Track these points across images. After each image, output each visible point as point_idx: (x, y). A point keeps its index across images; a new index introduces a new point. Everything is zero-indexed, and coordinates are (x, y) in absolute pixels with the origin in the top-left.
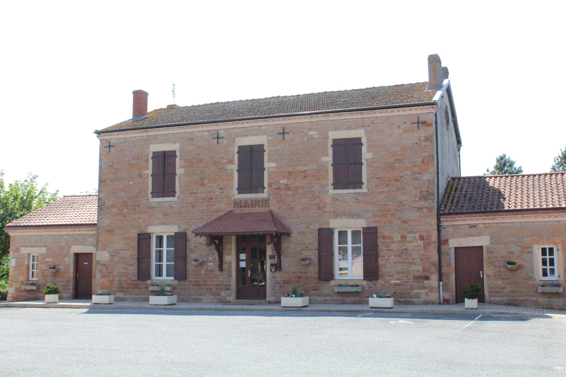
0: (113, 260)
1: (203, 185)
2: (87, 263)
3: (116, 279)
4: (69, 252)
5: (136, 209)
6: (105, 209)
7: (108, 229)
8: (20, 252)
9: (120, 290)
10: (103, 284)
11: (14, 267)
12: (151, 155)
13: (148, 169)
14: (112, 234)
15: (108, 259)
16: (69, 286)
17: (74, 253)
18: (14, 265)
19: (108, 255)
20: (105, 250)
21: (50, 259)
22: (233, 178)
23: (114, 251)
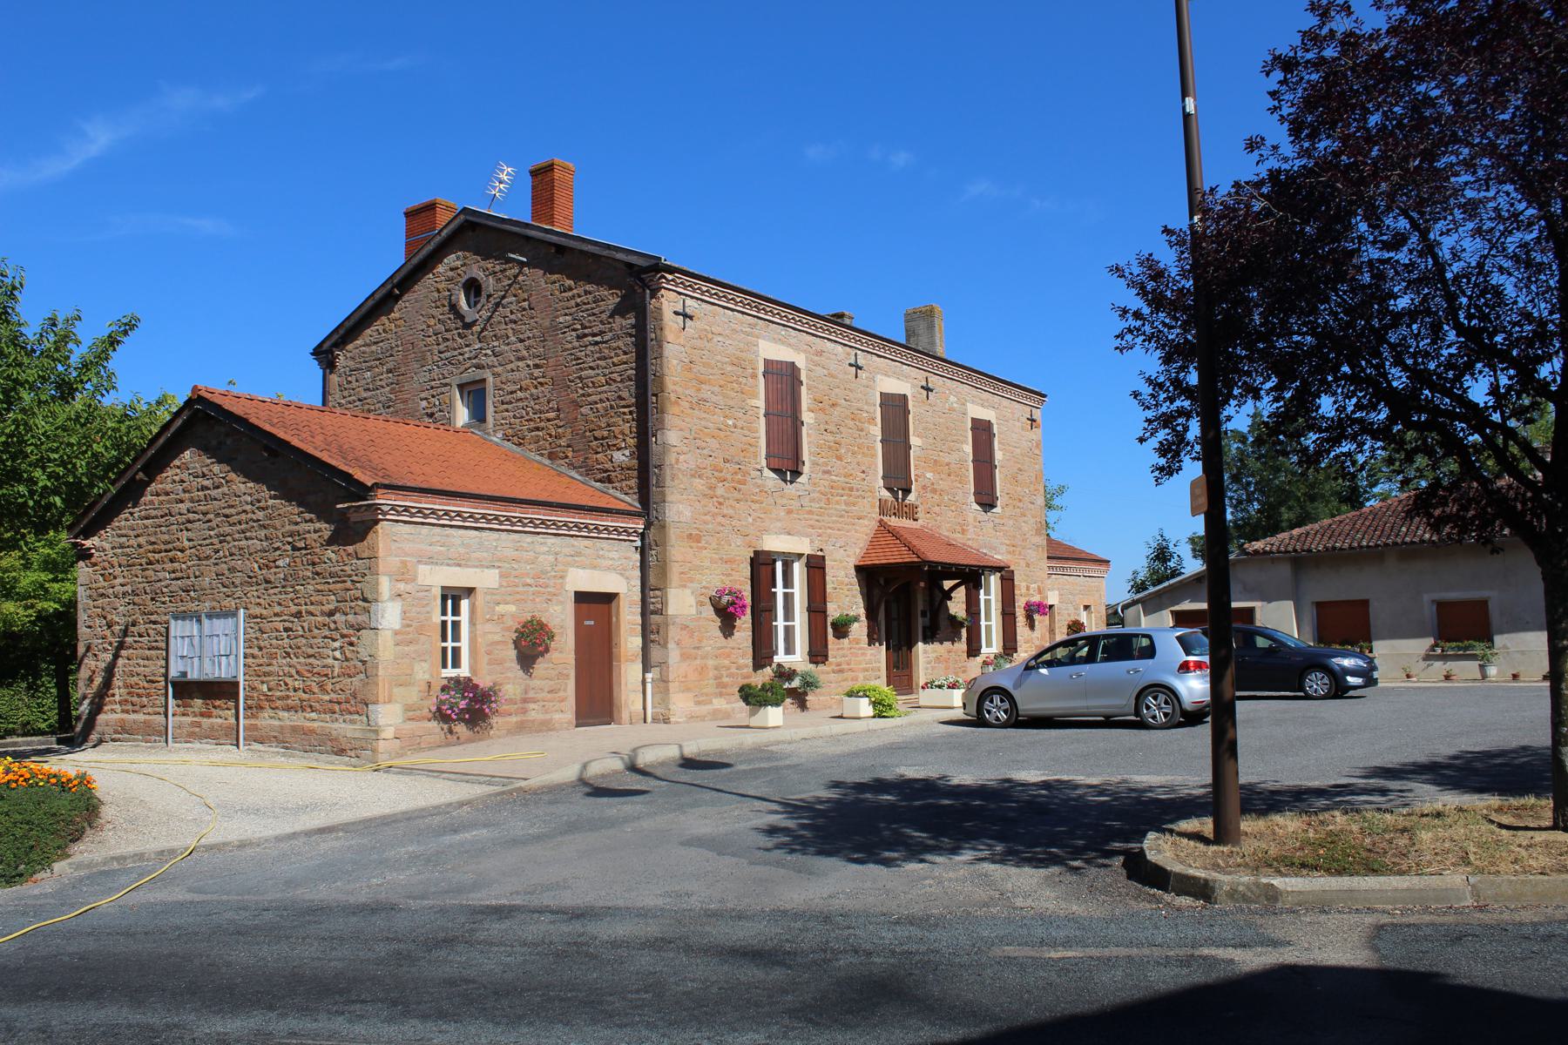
0: (702, 616)
1: (839, 458)
2: (592, 623)
3: (711, 663)
4: (562, 585)
5: (739, 491)
6: (681, 476)
7: (690, 531)
8: (414, 580)
9: (717, 691)
10: (686, 677)
11: (396, 633)
12: (761, 369)
13: (755, 396)
14: (698, 547)
15: (693, 611)
16: (565, 690)
17: (576, 592)
18: (397, 627)
19: (691, 600)
20: (685, 586)
21: (512, 608)
22: (874, 456)
23: (703, 590)
